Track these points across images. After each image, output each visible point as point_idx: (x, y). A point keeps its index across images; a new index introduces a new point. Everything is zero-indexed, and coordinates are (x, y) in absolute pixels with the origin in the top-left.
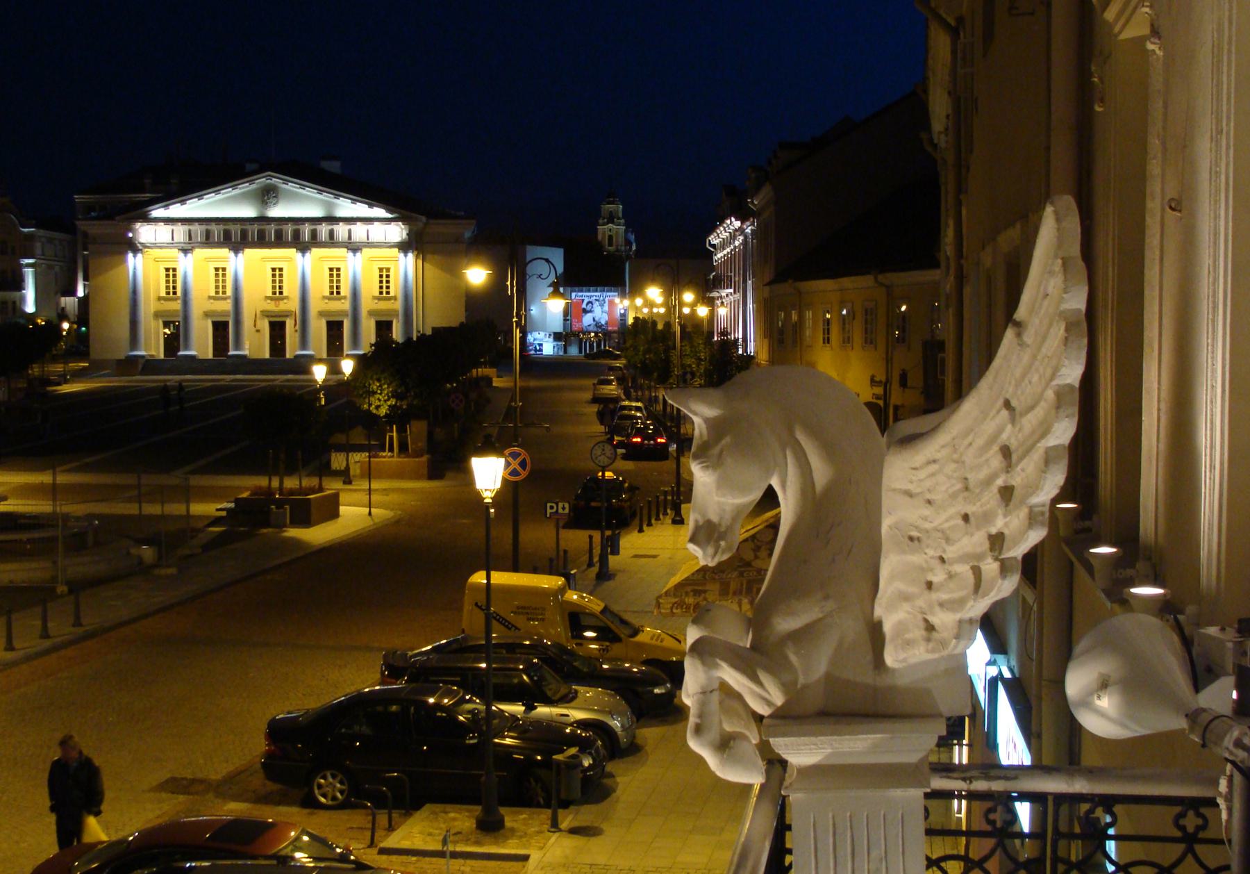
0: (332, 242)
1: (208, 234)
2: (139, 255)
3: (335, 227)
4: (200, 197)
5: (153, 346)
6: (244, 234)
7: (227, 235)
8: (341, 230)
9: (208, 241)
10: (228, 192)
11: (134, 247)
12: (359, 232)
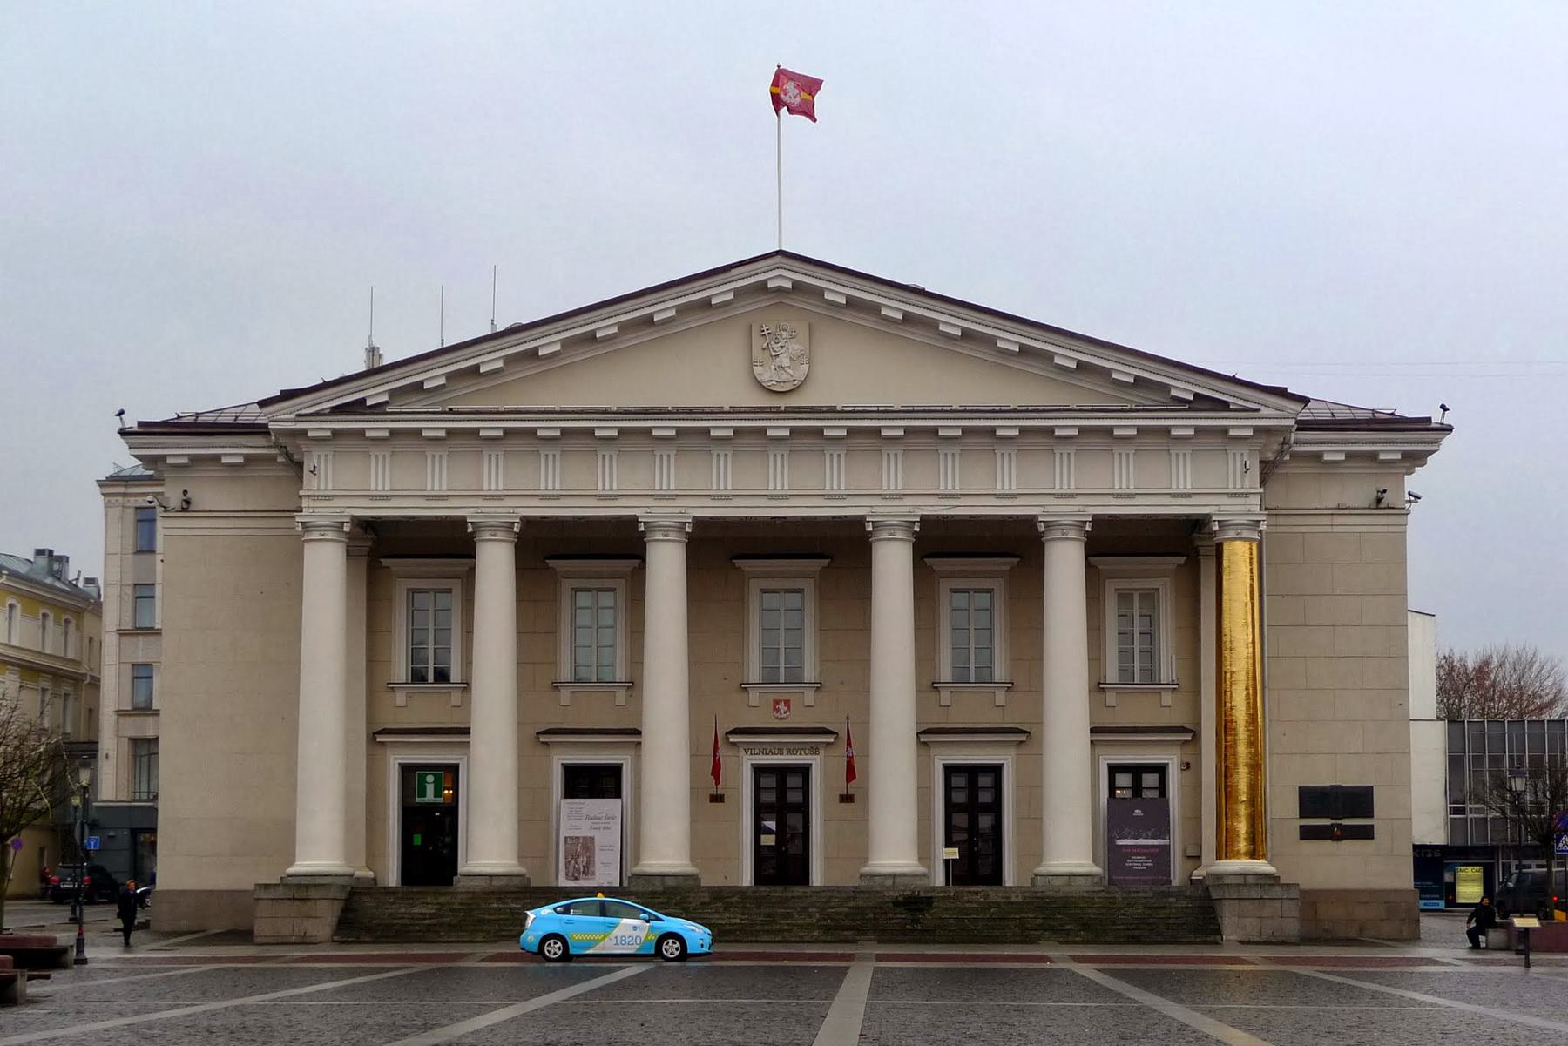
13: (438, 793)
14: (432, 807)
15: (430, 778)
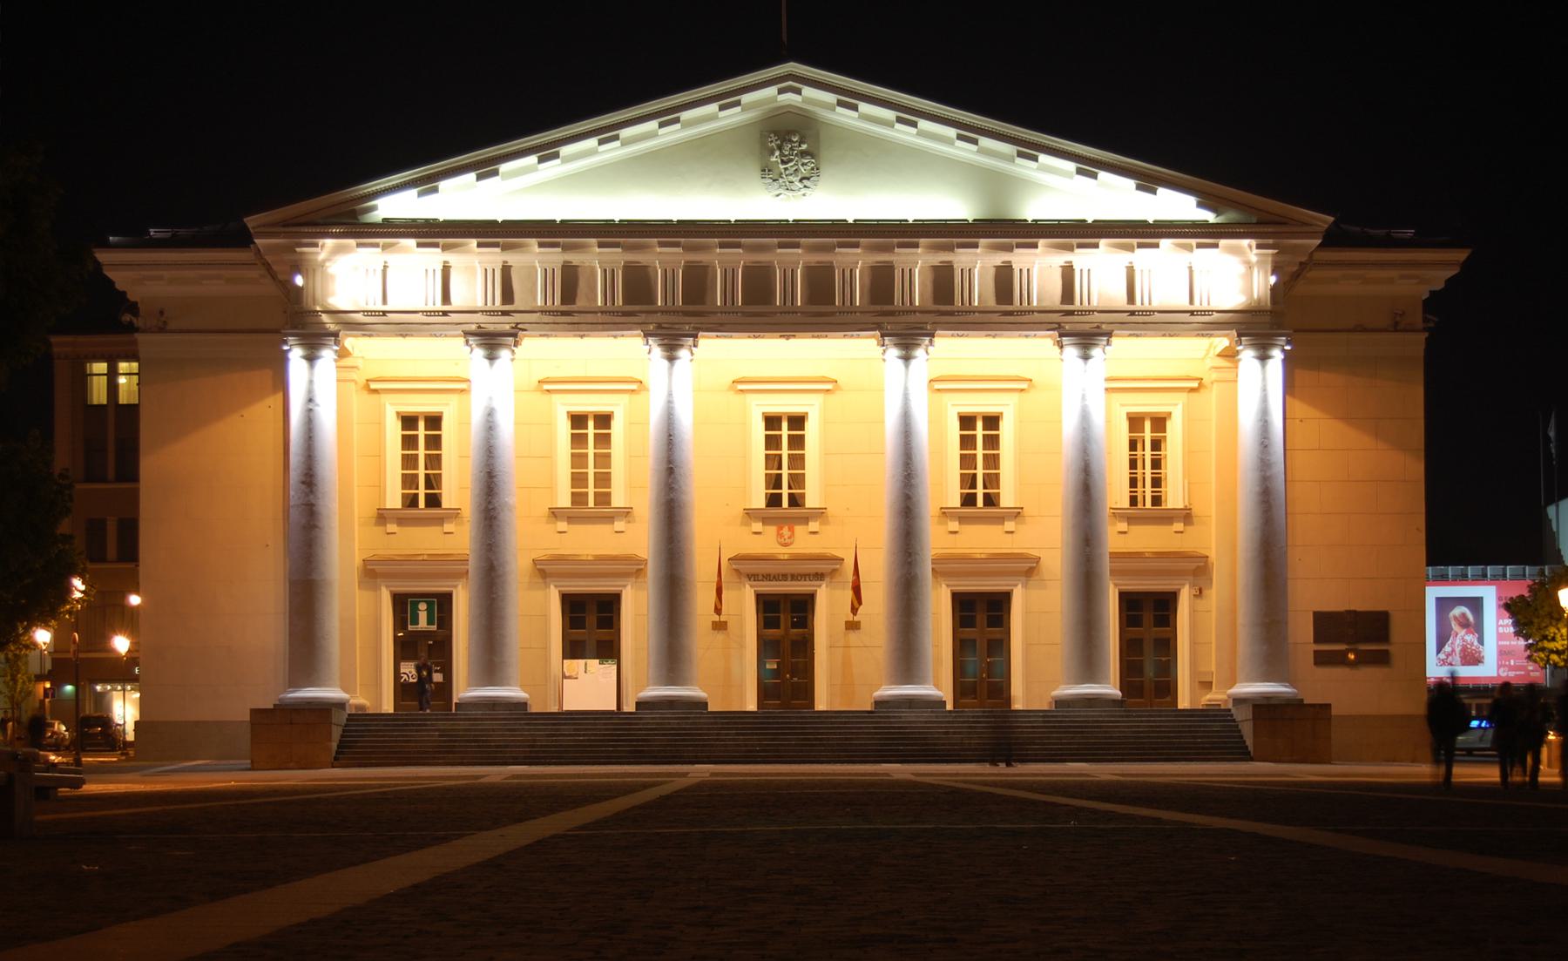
0: (1007, 311)
1: (570, 281)
2: (327, 355)
3: (1021, 259)
4: (547, 153)
5: (360, 672)
6: (697, 282)
7: (637, 287)
8: (1040, 268)
9: (571, 309)
10: (645, 135)
11: (312, 328)
12: (1103, 273)
13: (430, 622)
14: (425, 634)
15: (422, 606)
